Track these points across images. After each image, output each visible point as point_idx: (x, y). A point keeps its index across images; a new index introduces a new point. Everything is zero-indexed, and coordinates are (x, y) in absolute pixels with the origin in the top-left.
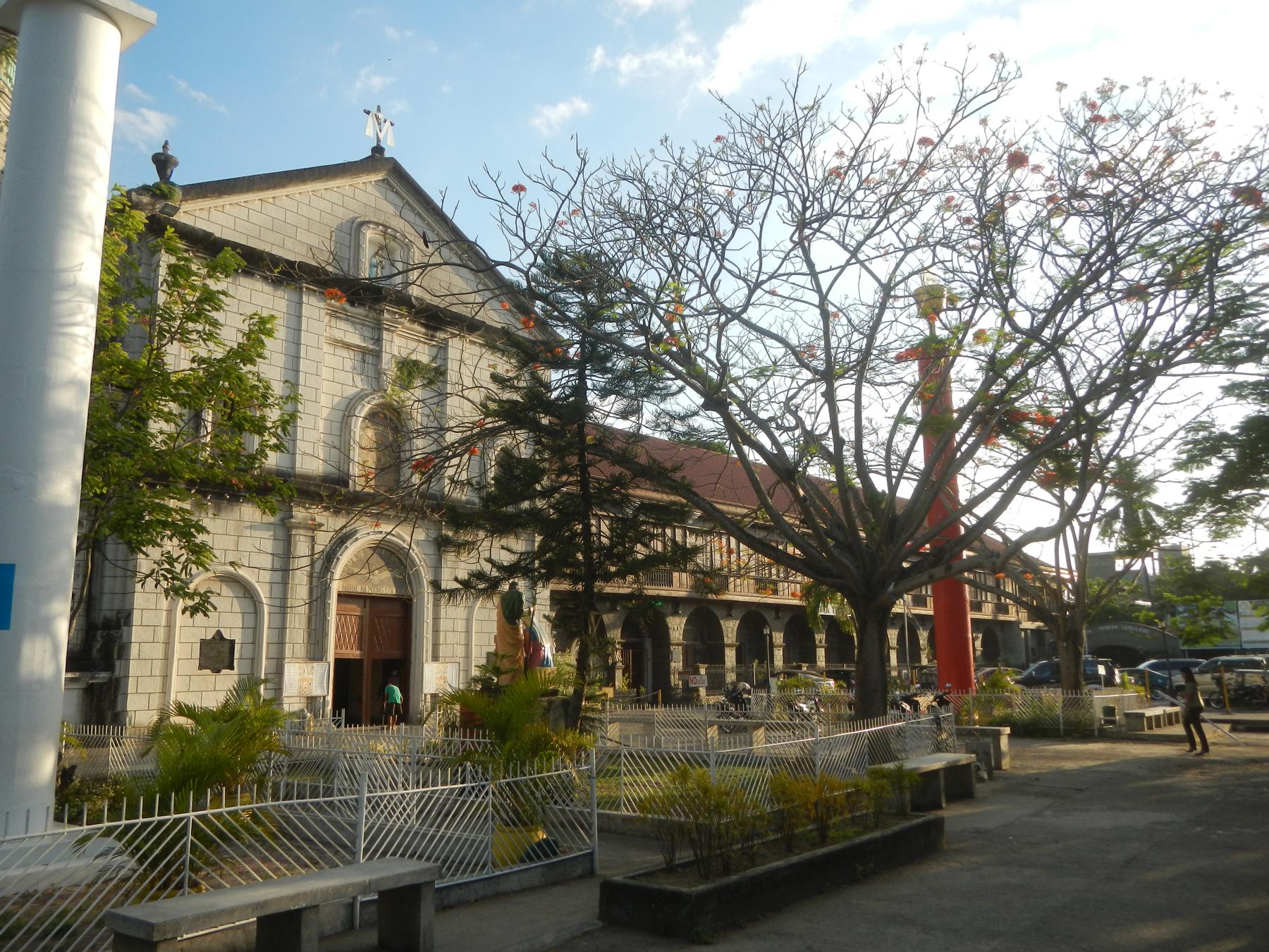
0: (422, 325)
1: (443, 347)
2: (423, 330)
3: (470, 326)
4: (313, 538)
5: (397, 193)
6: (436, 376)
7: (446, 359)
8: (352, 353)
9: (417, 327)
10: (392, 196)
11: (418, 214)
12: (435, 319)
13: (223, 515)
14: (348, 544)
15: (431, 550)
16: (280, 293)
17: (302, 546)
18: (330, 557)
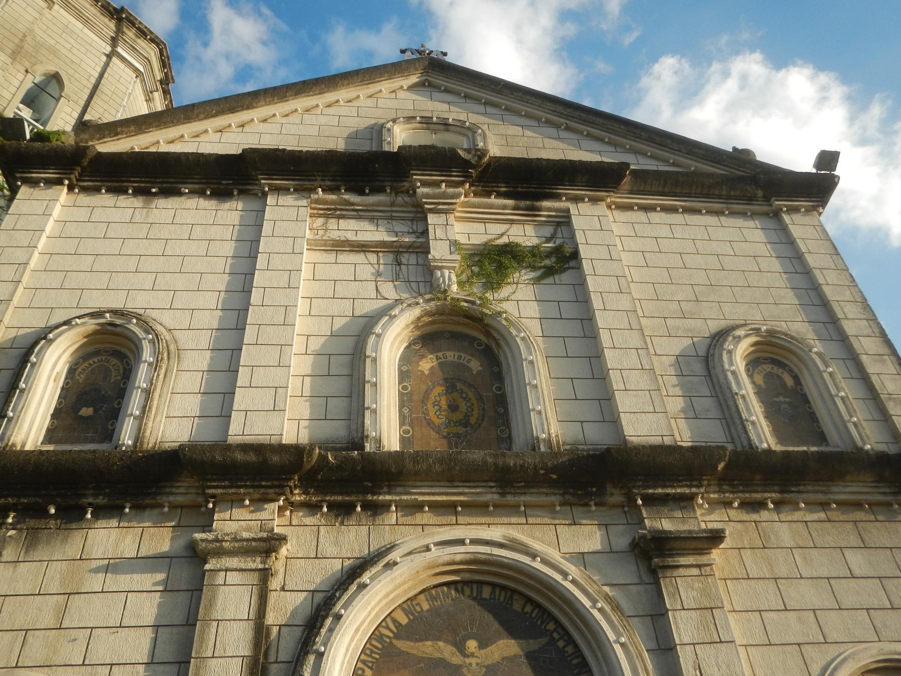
0: (506, 195)
1: (564, 221)
2: (510, 202)
3: (599, 179)
4: (265, 575)
5: (447, 91)
6: (560, 260)
7: (573, 237)
8: (372, 258)
9: (493, 200)
10: (436, 95)
11: (487, 103)
12: (525, 182)
13: (41, 553)
14: (365, 578)
15: (627, 572)
16: (227, 205)
17: (231, 596)
18: (321, 613)
